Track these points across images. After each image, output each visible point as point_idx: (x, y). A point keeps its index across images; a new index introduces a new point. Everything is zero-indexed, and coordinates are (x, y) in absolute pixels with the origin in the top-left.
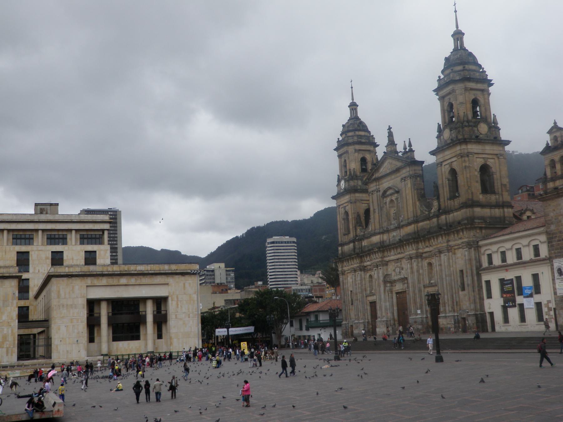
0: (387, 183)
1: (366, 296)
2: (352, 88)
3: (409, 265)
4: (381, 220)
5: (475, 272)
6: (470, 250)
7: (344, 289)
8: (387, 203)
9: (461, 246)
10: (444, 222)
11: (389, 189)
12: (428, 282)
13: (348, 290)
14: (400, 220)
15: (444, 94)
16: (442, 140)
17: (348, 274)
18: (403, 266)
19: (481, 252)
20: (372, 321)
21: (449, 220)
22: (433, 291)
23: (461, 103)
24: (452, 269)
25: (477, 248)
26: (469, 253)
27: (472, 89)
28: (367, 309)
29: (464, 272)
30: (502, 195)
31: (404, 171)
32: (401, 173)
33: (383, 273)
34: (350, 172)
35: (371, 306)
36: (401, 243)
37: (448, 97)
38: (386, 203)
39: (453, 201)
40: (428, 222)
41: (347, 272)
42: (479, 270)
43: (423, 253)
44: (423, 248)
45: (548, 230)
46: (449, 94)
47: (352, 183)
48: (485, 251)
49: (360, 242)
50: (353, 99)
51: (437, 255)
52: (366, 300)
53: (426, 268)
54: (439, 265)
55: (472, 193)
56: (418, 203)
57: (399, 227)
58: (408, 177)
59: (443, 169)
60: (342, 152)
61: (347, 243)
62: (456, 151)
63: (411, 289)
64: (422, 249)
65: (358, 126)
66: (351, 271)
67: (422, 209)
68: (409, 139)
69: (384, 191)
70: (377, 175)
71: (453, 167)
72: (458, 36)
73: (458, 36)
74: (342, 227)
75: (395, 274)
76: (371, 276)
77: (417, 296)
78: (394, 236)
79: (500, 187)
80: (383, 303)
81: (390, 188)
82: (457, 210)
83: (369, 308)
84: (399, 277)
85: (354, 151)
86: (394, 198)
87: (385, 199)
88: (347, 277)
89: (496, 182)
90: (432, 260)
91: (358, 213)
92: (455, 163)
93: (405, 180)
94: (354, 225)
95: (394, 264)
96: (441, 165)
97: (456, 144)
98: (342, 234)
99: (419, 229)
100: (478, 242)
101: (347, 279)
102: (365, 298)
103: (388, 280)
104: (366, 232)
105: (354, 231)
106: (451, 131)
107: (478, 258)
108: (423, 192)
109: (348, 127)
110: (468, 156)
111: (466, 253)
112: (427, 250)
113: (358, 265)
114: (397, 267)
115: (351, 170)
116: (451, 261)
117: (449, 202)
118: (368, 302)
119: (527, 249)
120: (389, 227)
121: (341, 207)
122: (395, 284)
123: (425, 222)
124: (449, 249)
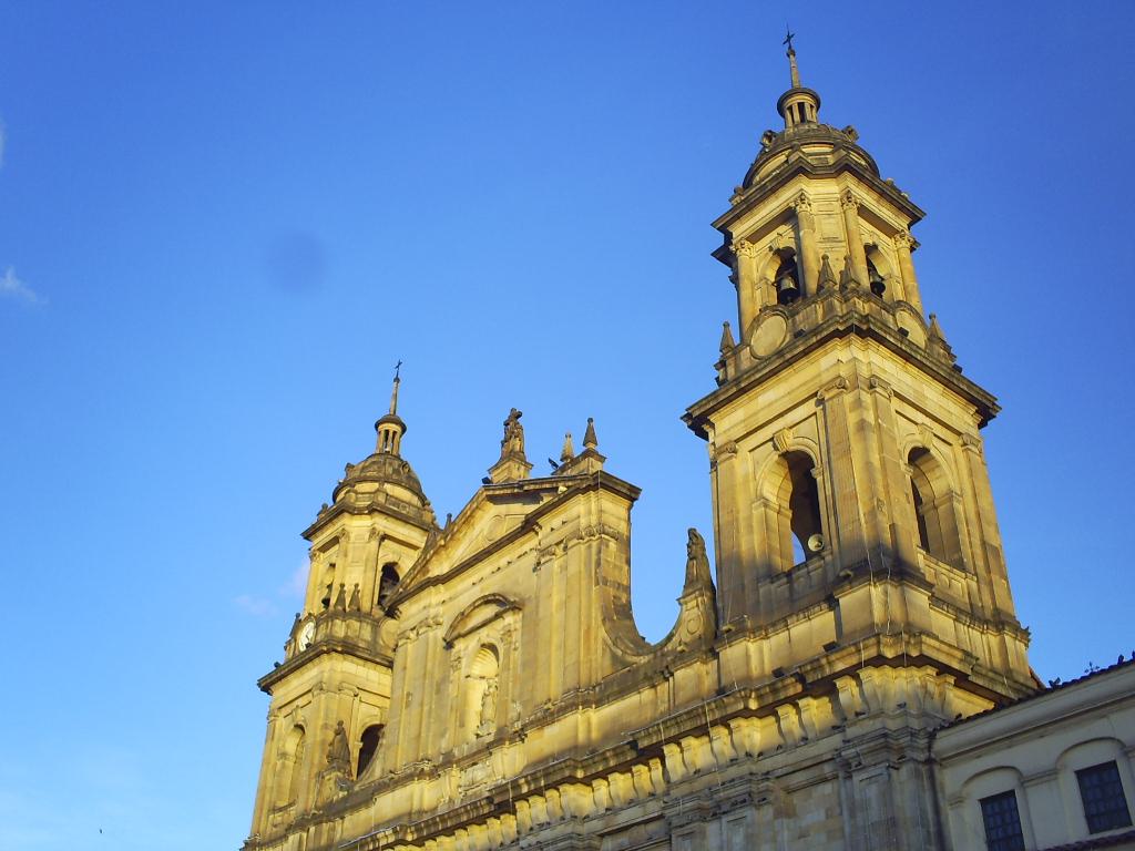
2: (397, 380)
4: (428, 729)
6: (894, 772)
10: (741, 672)
11: (478, 607)
15: (761, 224)
19: (943, 792)
21: (762, 662)
23: (828, 240)
25: (924, 769)
27: (863, 211)
30: (990, 584)
34: (342, 592)
40: (647, 694)
43: (602, 836)
47: (340, 629)
51: (686, 830)
55: (893, 527)
61: (275, 840)
65: (396, 471)
67: (620, 653)
68: (590, 420)
69: (463, 614)
70: (439, 568)
71: (792, 448)
79: (978, 551)
81: (487, 601)
85: (367, 536)
89: (963, 528)
91: (340, 723)
94: (315, 770)
97: (822, 343)
99: (595, 735)
100: (932, 736)
104: (357, 788)
107: (930, 815)
108: (624, 601)
110: (872, 387)
111: (873, 791)
115: (345, 588)
120: (456, 752)
123: (633, 700)
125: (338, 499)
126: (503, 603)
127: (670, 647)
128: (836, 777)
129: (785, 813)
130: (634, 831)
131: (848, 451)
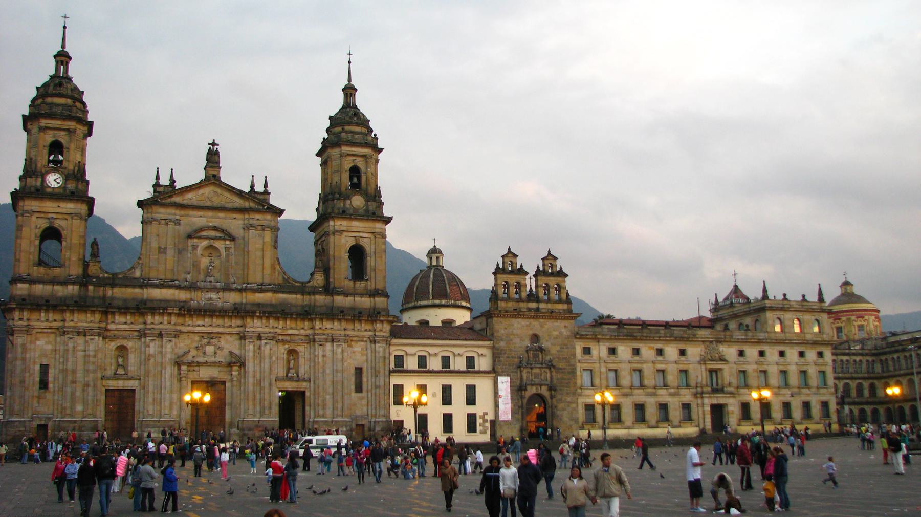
0: (205, 219)
1: (102, 379)
2: (65, 27)
3: (251, 347)
5: (387, 373)
7: (24, 359)
8: (199, 249)
9: (365, 339)
12: (282, 373)
13: (34, 363)
14: (232, 280)
16: (348, 206)
17: (38, 335)
18: (223, 343)
20: (105, 420)
22: (292, 388)
24: (345, 364)
26: (384, 352)
28: (100, 400)
29: (365, 370)
31: (257, 216)
32: (247, 216)
33: (173, 350)
35: (106, 397)
36: (240, 312)
37: (354, 158)
38: (198, 246)
39: (354, 283)
40: (299, 297)
41: (40, 330)
42: (390, 372)
43: (279, 334)
44: (297, 329)
45: (497, 345)
46: (364, 156)
48: (395, 351)
49: (102, 288)
50: (63, 46)
52: (102, 384)
53: (285, 356)
54: (324, 356)
56: (278, 267)
57: (227, 289)
58: (268, 227)
59: (343, 240)
60: (58, 126)
62: (375, 228)
63: (251, 380)
64: (281, 329)
66: (64, 332)
68: (266, 177)
70: (177, 199)
72: (349, 91)
73: (349, 91)
74: (32, 249)
75: (202, 355)
76: (122, 349)
77: (267, 391)
78: (210, 299)
80: (168, 396)
81: (215, 228)
82: (362, 295)
83: (103, 398)
84: (212, 359)
86: (219, 244)
87: (195, 240)
88: (37, 339)
90: (299, 347)
92: (365, 240)
93: (256, 230)
94: (81, 257)
95: (197, 339)
96: (341, 234)
98: (31, 263)
101: (35, 343)
102: (99, 382)
103: (185, 359)
105: (81, 266)
106: (367, 201)
109: (72, 90)
111: (381, 349)
112: (290, 332)
113: (97, 325)
114: (209, 343)
116: (346, 354)
117: (346, 282)
118: (104, 389)
119: (458, 359)
121: (38, 215)
122: (196, 368)
123: (294, 296)
124: (348, 340)
125: (49, 100)
126: (228, 236)
127: (309, 284)
128: (366, 341)
129: (350, 346)
130: (292, 337)
131: (382, 257)
